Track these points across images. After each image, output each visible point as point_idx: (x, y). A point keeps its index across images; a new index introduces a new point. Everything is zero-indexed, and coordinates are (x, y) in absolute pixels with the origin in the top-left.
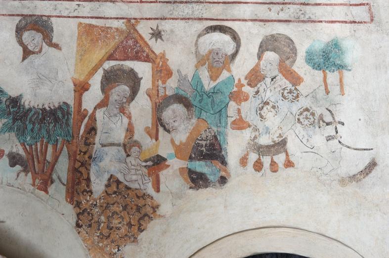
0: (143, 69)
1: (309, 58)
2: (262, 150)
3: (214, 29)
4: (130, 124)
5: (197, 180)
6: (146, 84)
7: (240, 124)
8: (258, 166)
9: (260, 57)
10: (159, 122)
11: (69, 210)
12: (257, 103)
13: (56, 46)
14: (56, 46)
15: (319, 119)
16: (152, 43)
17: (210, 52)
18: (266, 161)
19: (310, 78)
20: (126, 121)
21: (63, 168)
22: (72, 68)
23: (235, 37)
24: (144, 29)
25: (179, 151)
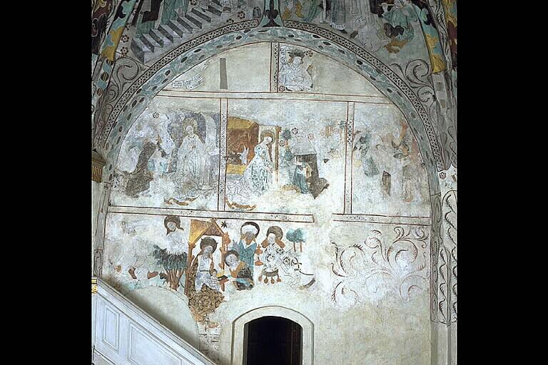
0: (218, 239)
1: (288, 237)
2: (267, 274)
3: (248, 223)
4: (212, 262)
5: (240, 286)
6: (219, 246)
7: (259, 263)
8: (266, 281)
9: (267, 235)
10: (224, 261)
11: (185, 297)
12: (266, 255)
13: (182, 229)
14: (182, 229)
15: (291, 262)
16: (222, 228)
17: (247, 233)
18: (269, 278)
19: (288, 245)
20: (211, 261)
21: (183, 280)
22: (188, 238)
23: (257, 226)
24: (219, 223)
25: (233, 274)
